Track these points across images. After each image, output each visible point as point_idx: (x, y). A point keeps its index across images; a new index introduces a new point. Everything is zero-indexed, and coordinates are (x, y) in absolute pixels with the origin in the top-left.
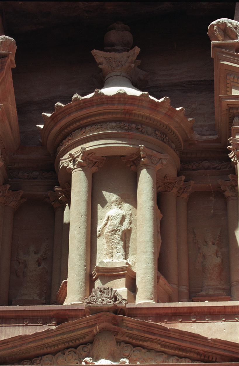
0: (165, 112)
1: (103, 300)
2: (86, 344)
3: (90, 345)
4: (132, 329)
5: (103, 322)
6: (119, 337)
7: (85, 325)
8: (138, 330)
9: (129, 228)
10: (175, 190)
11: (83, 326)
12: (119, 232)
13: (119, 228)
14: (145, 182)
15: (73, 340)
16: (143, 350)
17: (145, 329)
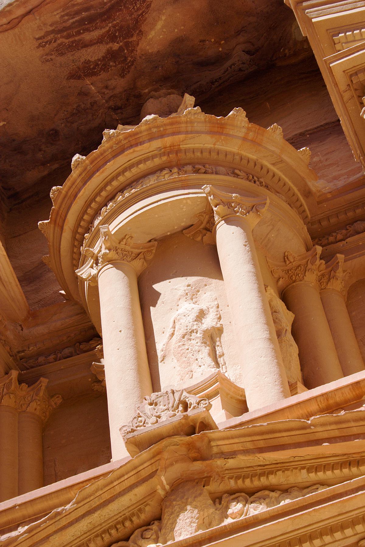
0: (241, 135)
1: (159, 417)
2: (148, 524)
3: (156, 522)
4: (232, 454)
5: (172, 464)
6: (214, 487)
7: (133, 480)
8: (246, 452)
9: (218, 325)
10: (311, 278)
11: (127, 484)
12: (197, 332)
13: (195, 327)
14: (230, 240)
15: (118, 523)
16: (272, 494)
17: (262, 444)
